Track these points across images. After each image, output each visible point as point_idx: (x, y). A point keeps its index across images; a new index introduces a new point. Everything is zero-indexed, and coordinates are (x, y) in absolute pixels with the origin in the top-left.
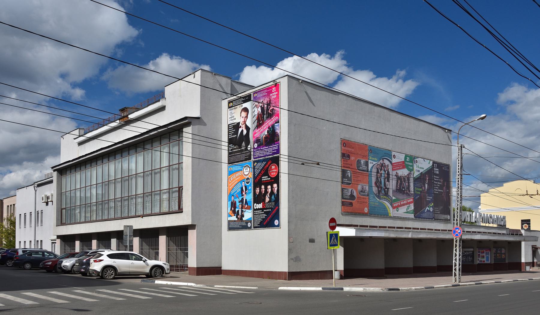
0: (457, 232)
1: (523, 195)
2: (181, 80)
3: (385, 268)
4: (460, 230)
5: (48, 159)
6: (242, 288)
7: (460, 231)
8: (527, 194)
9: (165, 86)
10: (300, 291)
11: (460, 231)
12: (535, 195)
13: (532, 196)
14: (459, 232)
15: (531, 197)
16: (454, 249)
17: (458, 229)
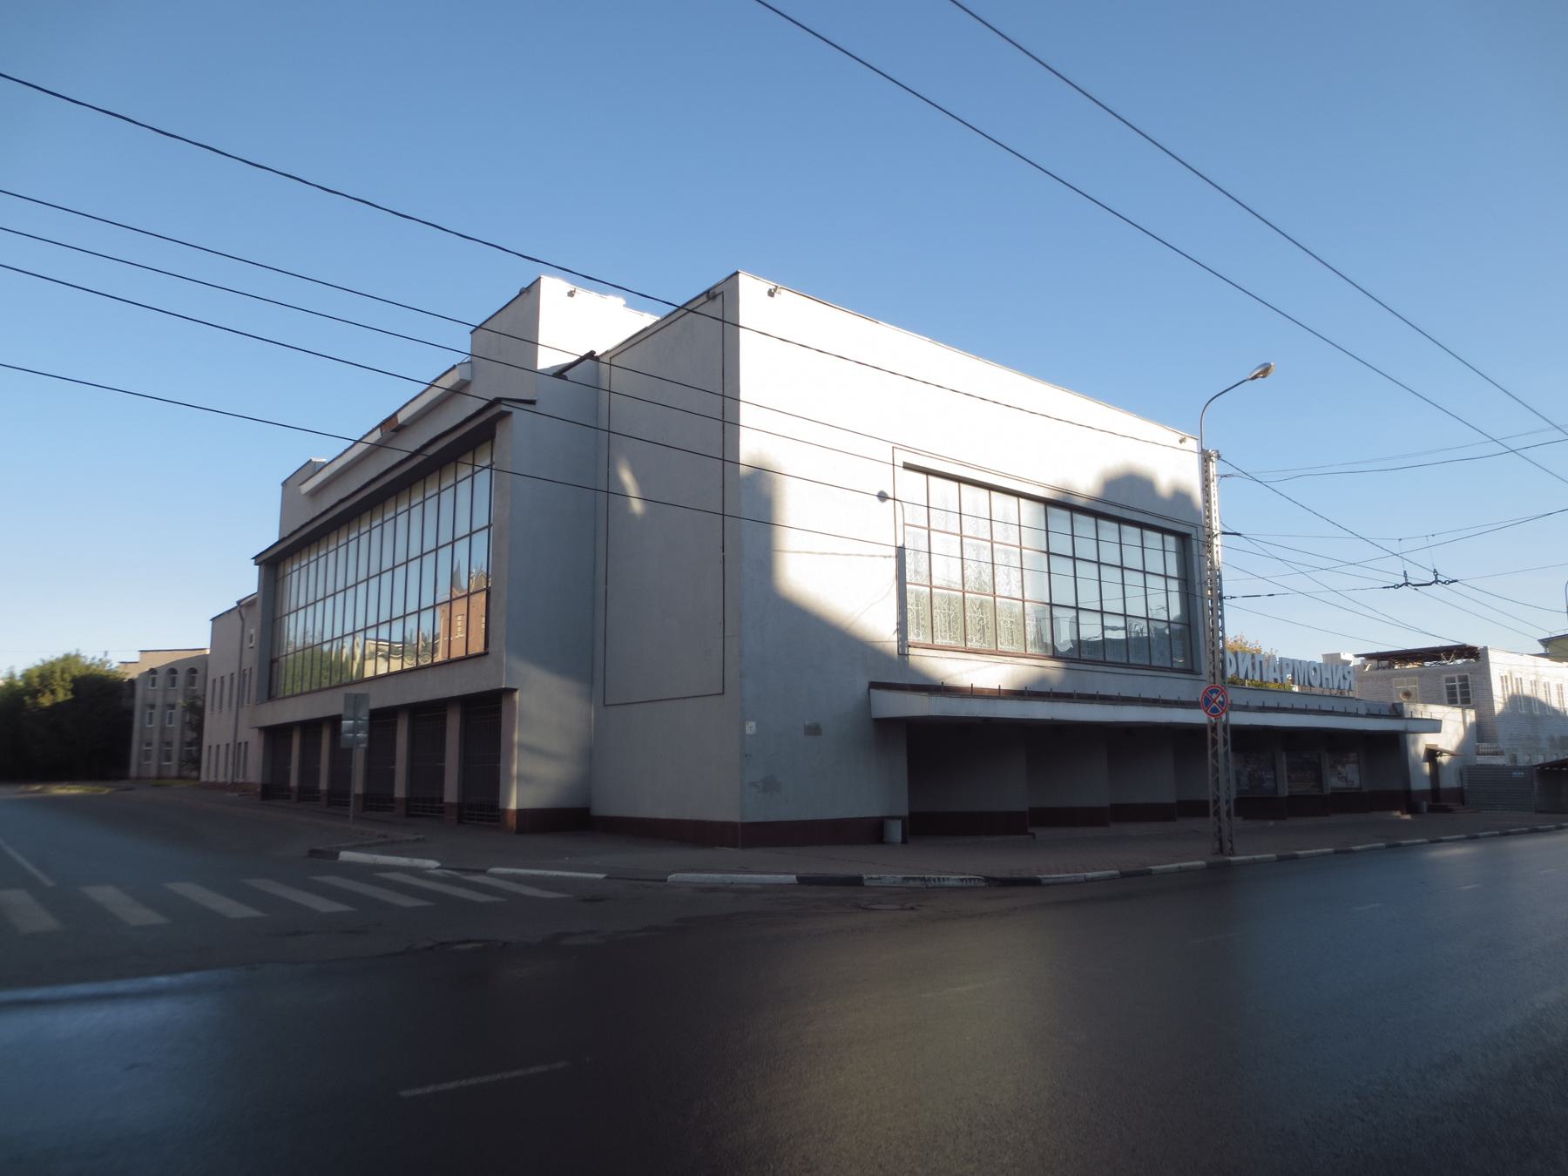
0: (1214, 701)
1: (1394, 587)
2: (357, 439)
3: (909, 814)
4: (1223, 696)
5: (90, 656)
6: (552, 876)
7: (1222, 699)
8: (1406, 584)
9: (301, 484)
10: (542, 877)
11: (1222, 699)
12: (1430, 584)
13: (1418, 588)
14: (1219, 701)
15: (1416, 589)
16: (1210, 752)
17: (1216, 692)
